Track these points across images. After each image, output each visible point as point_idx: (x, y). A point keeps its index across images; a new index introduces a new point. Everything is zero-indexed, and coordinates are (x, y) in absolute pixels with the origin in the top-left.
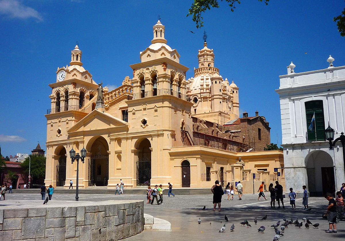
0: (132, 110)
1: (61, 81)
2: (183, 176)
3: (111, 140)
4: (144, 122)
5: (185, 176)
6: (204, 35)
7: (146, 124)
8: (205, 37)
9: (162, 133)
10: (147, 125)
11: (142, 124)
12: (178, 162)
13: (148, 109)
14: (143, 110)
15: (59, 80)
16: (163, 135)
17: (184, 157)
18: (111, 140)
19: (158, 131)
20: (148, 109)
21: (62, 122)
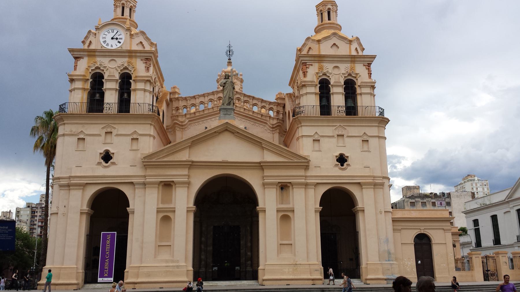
0: (313, 135)
1: (109, 47)
2: (417, 262)
3: (264, 185)
4: (342, 160)
5: (419, 262)
6: (228, 49)
7: (346, 163)
8: (230, 52)
9: (381, 181)
10: (348, 165)
11: (338, 163)
12: (410, 236)
13: (348, 136)
14: (336, 136)
15: (105, 45)
16: (382, 185)
17: (421, 228)
18: (265, 185)
19: (374, 177)
20: (348, 136)
21: (117, 135)
